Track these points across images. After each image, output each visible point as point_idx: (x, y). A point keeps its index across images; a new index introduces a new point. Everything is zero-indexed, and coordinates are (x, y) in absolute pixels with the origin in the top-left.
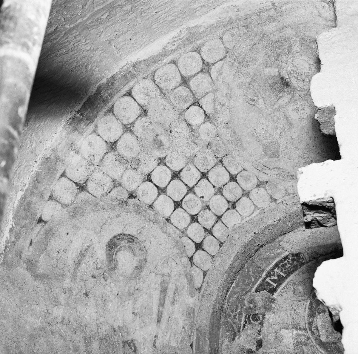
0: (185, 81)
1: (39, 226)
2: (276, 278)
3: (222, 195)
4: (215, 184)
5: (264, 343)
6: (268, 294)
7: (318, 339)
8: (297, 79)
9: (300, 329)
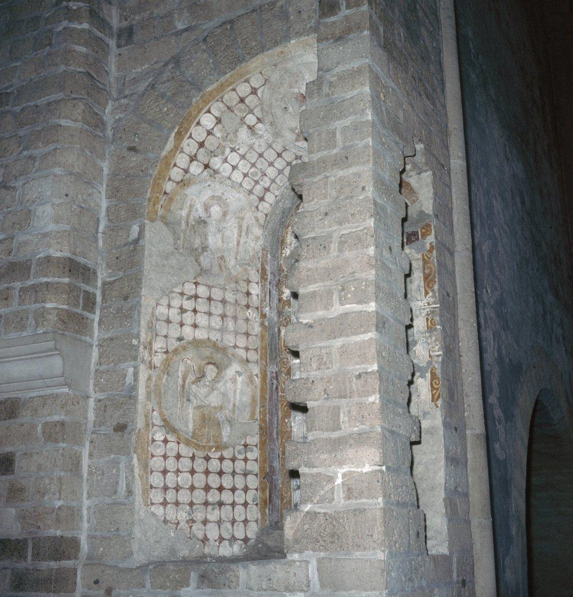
1: (165, 196)
3: (274, 166)
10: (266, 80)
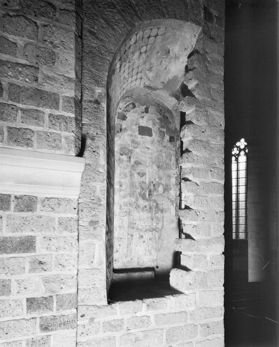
10: (165, 33)
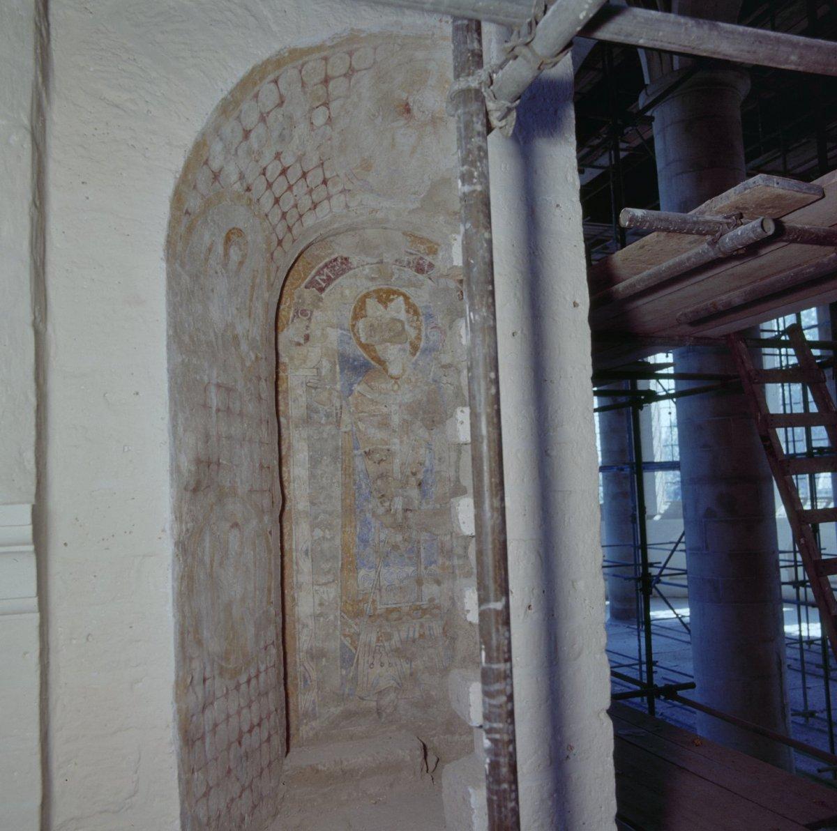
0: (326, 81)
2: (325, 278)
4: (310, 186)
5: (311, 338)
6: (317, 292)
7: (358, 339)
8: (418, 108)
9: (344, 330)
